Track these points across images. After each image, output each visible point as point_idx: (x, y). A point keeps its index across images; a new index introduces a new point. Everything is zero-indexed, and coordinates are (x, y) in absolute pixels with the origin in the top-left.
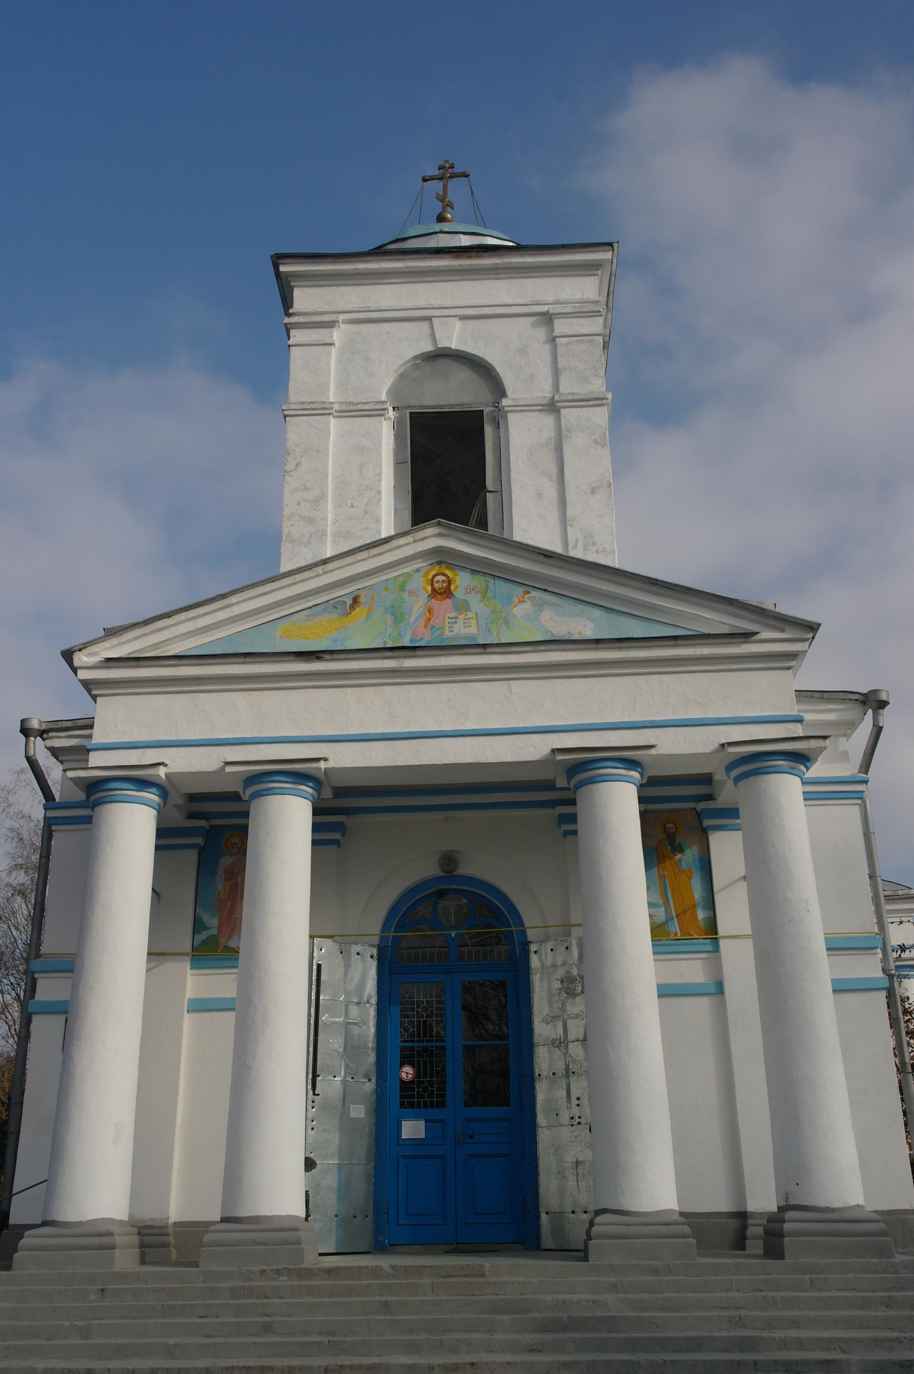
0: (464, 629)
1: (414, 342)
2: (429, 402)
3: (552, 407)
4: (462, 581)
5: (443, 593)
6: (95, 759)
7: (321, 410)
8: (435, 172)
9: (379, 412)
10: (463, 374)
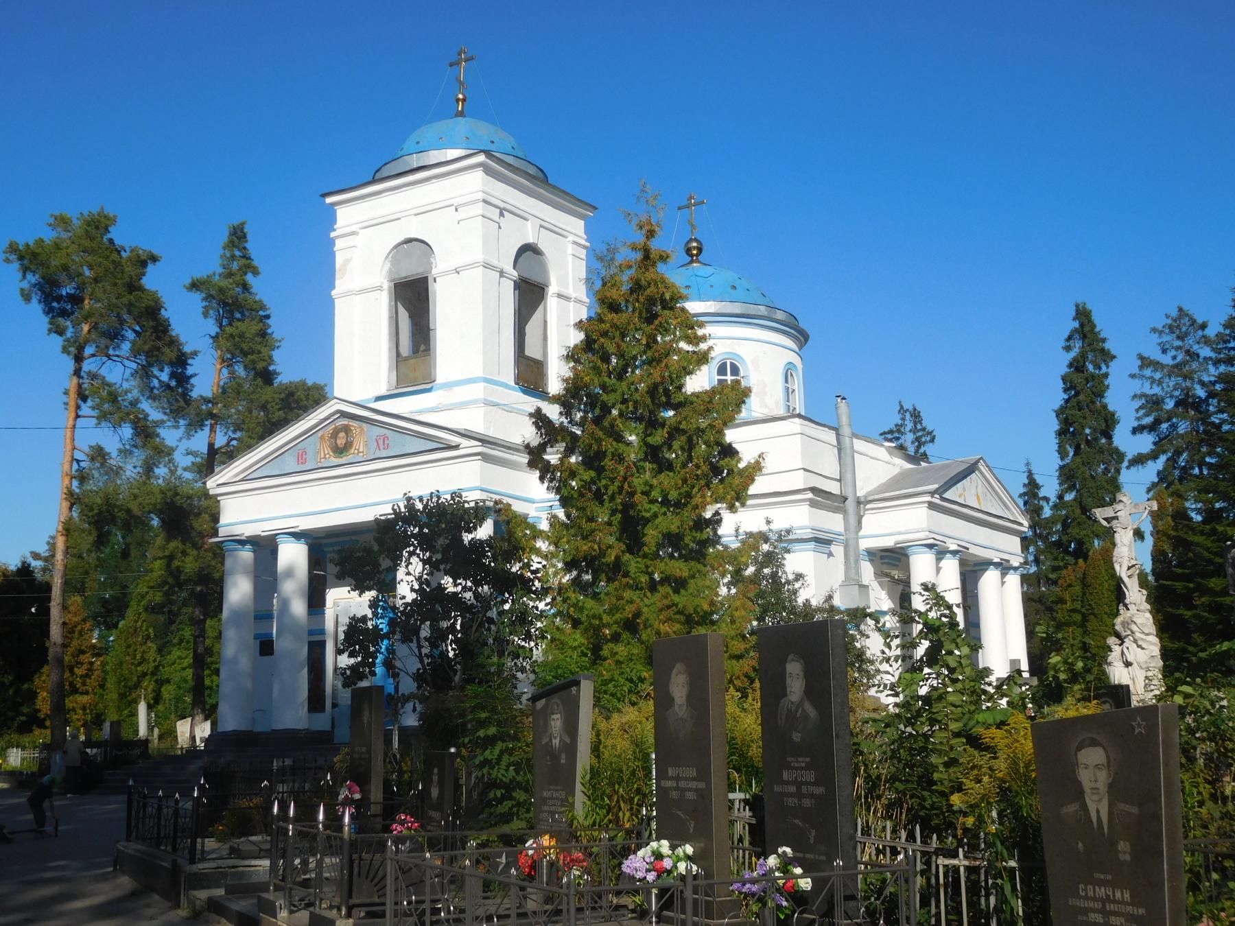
2: (403, 275)
9: (380, 288)
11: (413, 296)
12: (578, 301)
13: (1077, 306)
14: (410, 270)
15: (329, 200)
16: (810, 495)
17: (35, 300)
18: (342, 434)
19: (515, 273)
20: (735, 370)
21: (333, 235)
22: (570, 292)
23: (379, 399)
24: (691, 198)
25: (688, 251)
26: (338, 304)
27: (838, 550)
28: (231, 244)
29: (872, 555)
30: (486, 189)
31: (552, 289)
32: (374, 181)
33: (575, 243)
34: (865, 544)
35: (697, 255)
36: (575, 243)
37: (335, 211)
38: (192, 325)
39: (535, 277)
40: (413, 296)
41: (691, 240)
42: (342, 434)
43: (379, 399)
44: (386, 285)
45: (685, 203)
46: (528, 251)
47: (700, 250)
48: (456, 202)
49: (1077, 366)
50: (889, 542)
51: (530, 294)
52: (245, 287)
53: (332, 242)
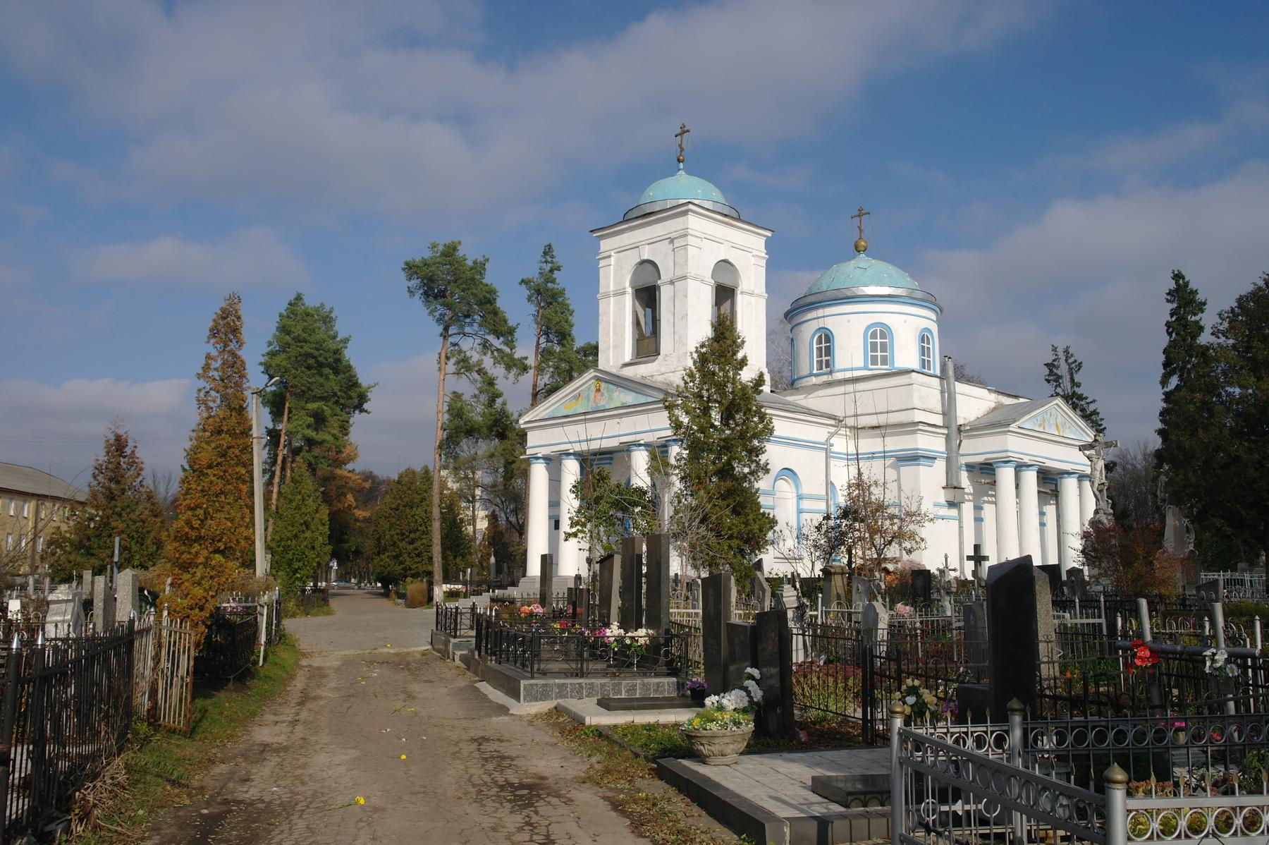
0: (603, 403)
1: (632, 260)
3: (672, 282)
4: (603, 385)
5: (598, 390)
6: (528, 452)
7: (607, 296)
8: (679, 131)
10: (650, 267)
11: (648, 296)
12: (758, 296)
14: (646, 281)
17: (417, 296)
23: (626, 365)
26: (602, 303)
27: (940, 465)
28: (545, 253)
29: (970, 467)
32: (625, 221)
34: (963, 460)
38: (518, 309)
39: (727, 282)
40: (648, 296)
43: (626, 365)
44: (629, 290)
46: (725, 265)
48: (672, 236)
50: (981, 459)
51: (724, 294)
52: (553, 281)
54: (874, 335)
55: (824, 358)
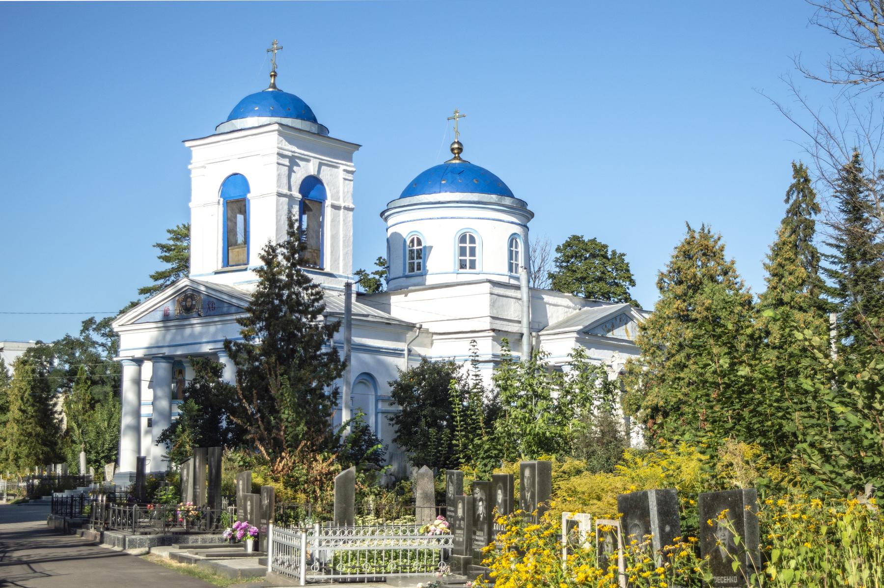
13: (794, 166)
14: (235, 194)
15: (187, 144)
16: (492, 334)
18: (189, 300)
19: (300, 196)
20: (472, 240)
21: (190, 167)
22: (342, 204)
23: (216, 273)
24: (456, 112)
25: (452, 150)
30: (280, 146)
31: (328, 203)
33: (345, 170)
35: (459, 153)
36: (345, 170)
37: (191, 151)
41: (455, 143)
42: (189, 300)
45: (452, 115)
47: (460, 150)
49: (795, 210)
53: (189, 171)
54: (463, 239)
55: (416, 261)
